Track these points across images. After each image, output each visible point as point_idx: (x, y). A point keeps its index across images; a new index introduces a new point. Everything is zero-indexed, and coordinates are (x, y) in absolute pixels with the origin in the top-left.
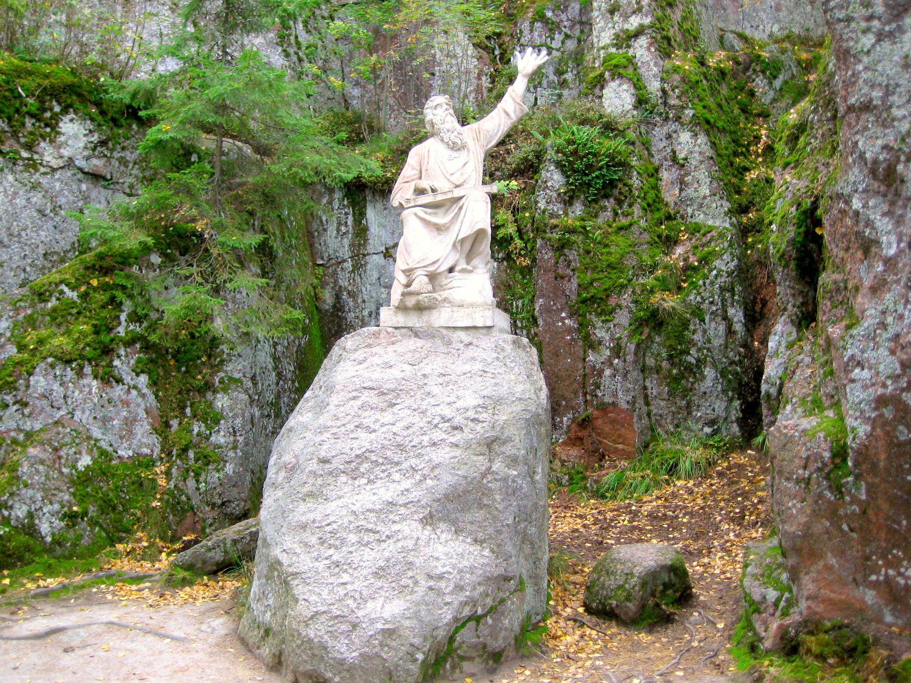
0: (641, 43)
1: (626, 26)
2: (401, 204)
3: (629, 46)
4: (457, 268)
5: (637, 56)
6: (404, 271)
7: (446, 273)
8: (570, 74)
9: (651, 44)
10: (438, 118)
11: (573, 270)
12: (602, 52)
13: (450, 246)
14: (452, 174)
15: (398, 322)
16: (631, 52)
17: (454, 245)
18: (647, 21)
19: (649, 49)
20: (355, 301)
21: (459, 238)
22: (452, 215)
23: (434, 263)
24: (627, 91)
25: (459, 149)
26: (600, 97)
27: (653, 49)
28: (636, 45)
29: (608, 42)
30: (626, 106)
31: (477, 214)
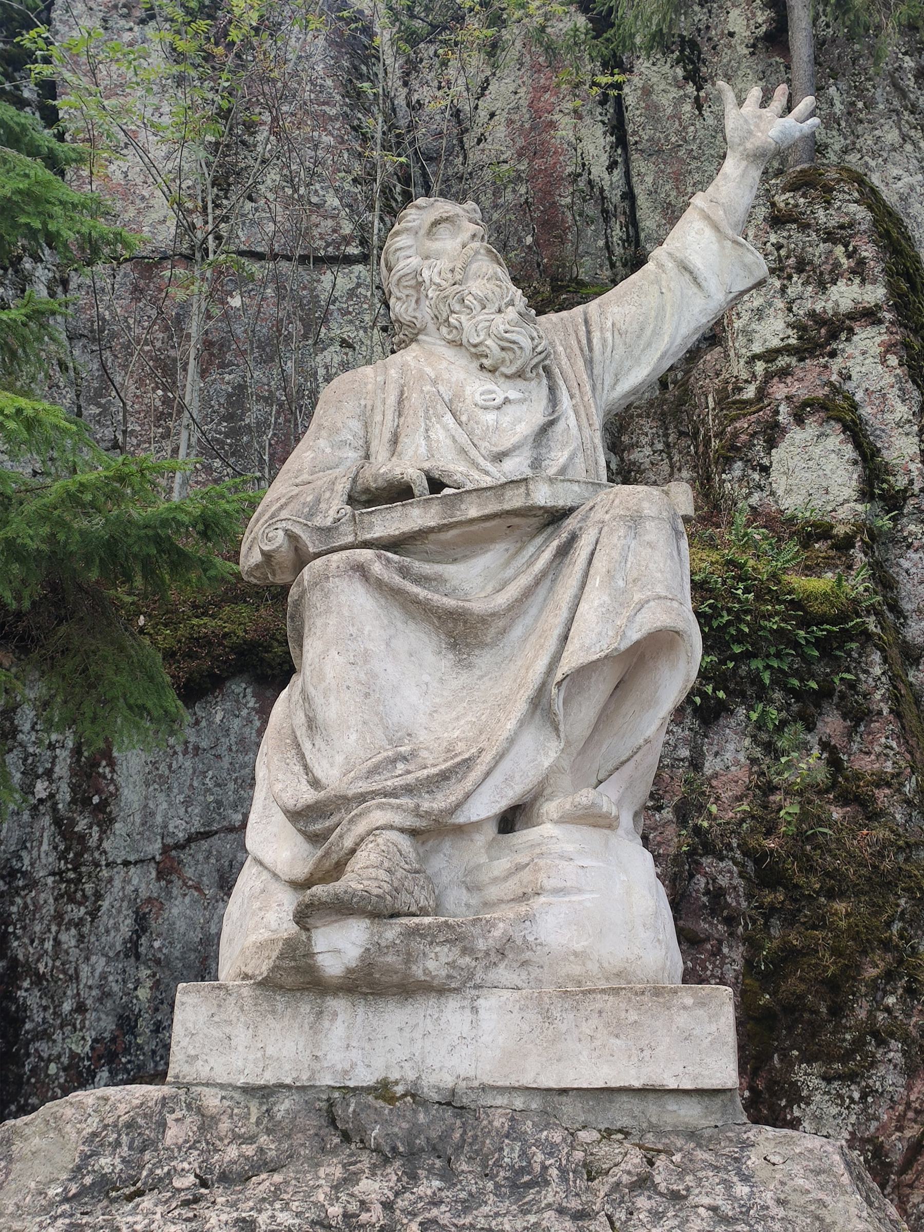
0: (862, 345)
1: (818, 308)
2: (292, 537)
3: (833, 354)
4: (550, 808)
5: (855, 376)
6: (300, 816)
7: (491, 830)
8: (648, 451)
9: (889, 348)
10: (443, 264)
11: (730, 921)
12: (760, 367)
13: (520, 706)
14: (499, 457)
15: (266, 1061)
16: (837, 364)
17: (539, 703)
18: (875, 294)
19: (884, 362)
20: (53, 998)
21: (570, 662)
22: (524, 580)
23: (444, 776)
24: (838, 452)
25: (520, 375)
26: (765, 470)
27: (893, 360)
28: (850, 350)
29: (775, 343)
30: (834, 490)
31: (636, 572)
